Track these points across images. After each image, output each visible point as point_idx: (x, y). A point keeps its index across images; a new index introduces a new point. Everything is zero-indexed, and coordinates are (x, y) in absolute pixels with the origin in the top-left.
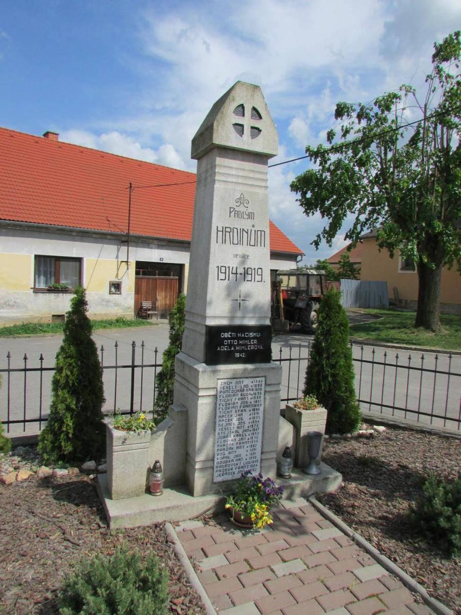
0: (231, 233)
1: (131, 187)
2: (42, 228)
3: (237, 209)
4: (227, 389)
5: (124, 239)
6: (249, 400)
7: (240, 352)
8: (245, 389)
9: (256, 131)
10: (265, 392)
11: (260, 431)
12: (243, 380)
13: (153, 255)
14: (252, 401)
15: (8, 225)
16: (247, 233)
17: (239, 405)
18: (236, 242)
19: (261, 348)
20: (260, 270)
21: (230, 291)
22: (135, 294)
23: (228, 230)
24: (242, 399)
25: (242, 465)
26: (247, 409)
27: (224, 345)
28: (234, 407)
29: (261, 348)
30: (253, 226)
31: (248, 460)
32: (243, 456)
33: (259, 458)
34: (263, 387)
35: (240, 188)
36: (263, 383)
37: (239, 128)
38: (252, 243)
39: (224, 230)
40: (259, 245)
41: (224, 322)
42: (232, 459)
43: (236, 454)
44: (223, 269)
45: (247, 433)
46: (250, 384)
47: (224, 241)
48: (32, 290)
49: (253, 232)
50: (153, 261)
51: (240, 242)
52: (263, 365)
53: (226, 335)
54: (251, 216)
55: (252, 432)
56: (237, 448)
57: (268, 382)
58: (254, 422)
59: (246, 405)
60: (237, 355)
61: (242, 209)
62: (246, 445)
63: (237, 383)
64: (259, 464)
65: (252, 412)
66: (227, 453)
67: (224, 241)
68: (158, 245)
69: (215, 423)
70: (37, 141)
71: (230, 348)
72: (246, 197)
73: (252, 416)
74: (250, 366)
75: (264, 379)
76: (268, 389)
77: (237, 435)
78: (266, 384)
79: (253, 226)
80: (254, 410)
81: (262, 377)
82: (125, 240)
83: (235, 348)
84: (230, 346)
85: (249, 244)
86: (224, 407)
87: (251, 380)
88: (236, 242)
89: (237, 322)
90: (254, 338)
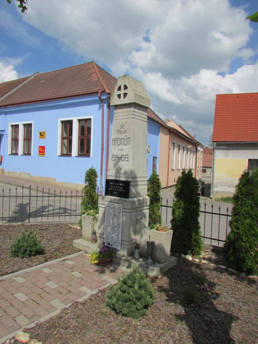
0: (118, 141)
2: (237, 144)
3: (120, 130)
4: (108, 206)
6: (117, 214)
7: (116, 191)
8: (115, 208)
11: (121, 229)
12: (114, 203)
15: (234, 144)
16: (123, 139)
17: (113, 214)
19: (124, 191)
20: (127, 156)
21: (115, 165)
23: (116, 139)
24: (114, 212)
25: (113, 242)
26: (116, 217)
27: (110, 188)
28: (111, 215)
29: (124, 191)
30: (126, 136)
31: (116, 241)
32: (114, 238)
33: (120, 241)
34: (122, 209)
35: (122, 120)
39: (116, 140)
40: (128, 144)
41: (113, 178)
42: (110, 237)
43: (112, 236)
45: (116, 228)
47: (115, 144)
49: (126, 139)
52: (124, 199)
53: (112, 183)
54: (125, 132)
55: (117, 228)
56: (112, 233)
57: (124, 207)
60: (115, 193)
61: (122, 129)
63: (112, 204)
64: (120, 244)
65: (117, 219)
66: (108, 234)
67: (115, 144)
69: (104, 219)
71: (113, 189)
73: (117, 221)
74: (118, 198)
75: (122, 205)
76: (124, 210)
77: (112, 228)
79: (126, 136)
80: (118, 218)
81: (122, 204)
83: (114, 189)
84: (113, 188)
86: (107, 214)
87: (117, 204)
89: (118, 179)
90: (122, 186)
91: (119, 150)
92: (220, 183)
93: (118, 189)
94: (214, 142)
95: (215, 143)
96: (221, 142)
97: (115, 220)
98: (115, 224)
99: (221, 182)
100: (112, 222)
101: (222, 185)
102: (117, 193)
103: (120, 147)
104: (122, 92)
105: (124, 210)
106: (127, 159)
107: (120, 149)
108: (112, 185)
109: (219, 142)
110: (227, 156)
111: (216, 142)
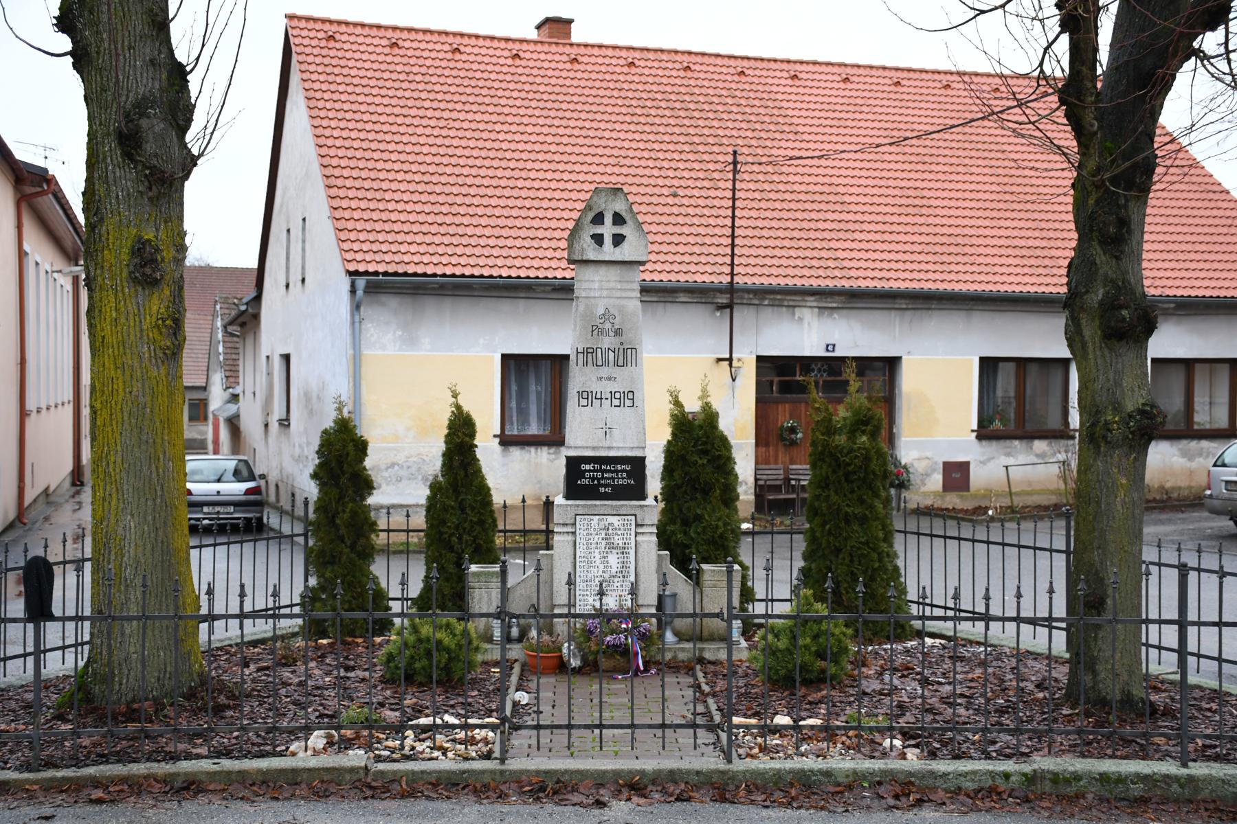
1: (735, 163)
5: (723, 299)
6: (616, 542)
7: (605, 486)
9: (618, 240)
10: (637, 534)
13: (806, 336)
14: (620, 542)
18: (600, 363)
20: (630, 396)
22: (757, 445)
30: (622, 344)
36: (633, 523)
37: (598, 239)
38: (621, 363)
44: (585, 395)
46: (616, 523)
47: (585, 364)
48: (498, 440)
50: (807, 352)
51: (605, 363)
53: (587, 467)
57: (640, 522)
58: (624, 566)
59: (612, 547)
60: (602, 490)
62: (614, 594)
67: (585, 364)
68: (819, 308)
70: (513, 47)
72: (612, 311)
76: (640, 530)
78: (637, 525)
79: (622, 344)
82: (727, 299)
85: (616, 364)
88: (600, 363)
91: (601, 379)
92: (388, 468)
93: (613, 479)
94: (351, 273)
95: (361, 282)
96: (386, 274)
97: (613, 560)
98: (614, 570)
99: (393, 465)
100: (601, 566)
101: (400, 480)
102: (609, 490)
103: (604, 372)
104: (608, 230)
105: (640, 530)
106: (628, 403)
107: (605, 375)
108: (590, 471)
109: (376, 273)
110: (411, 341)
111: (366, 273)
